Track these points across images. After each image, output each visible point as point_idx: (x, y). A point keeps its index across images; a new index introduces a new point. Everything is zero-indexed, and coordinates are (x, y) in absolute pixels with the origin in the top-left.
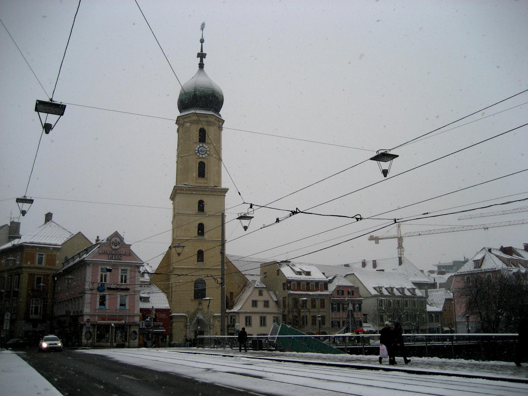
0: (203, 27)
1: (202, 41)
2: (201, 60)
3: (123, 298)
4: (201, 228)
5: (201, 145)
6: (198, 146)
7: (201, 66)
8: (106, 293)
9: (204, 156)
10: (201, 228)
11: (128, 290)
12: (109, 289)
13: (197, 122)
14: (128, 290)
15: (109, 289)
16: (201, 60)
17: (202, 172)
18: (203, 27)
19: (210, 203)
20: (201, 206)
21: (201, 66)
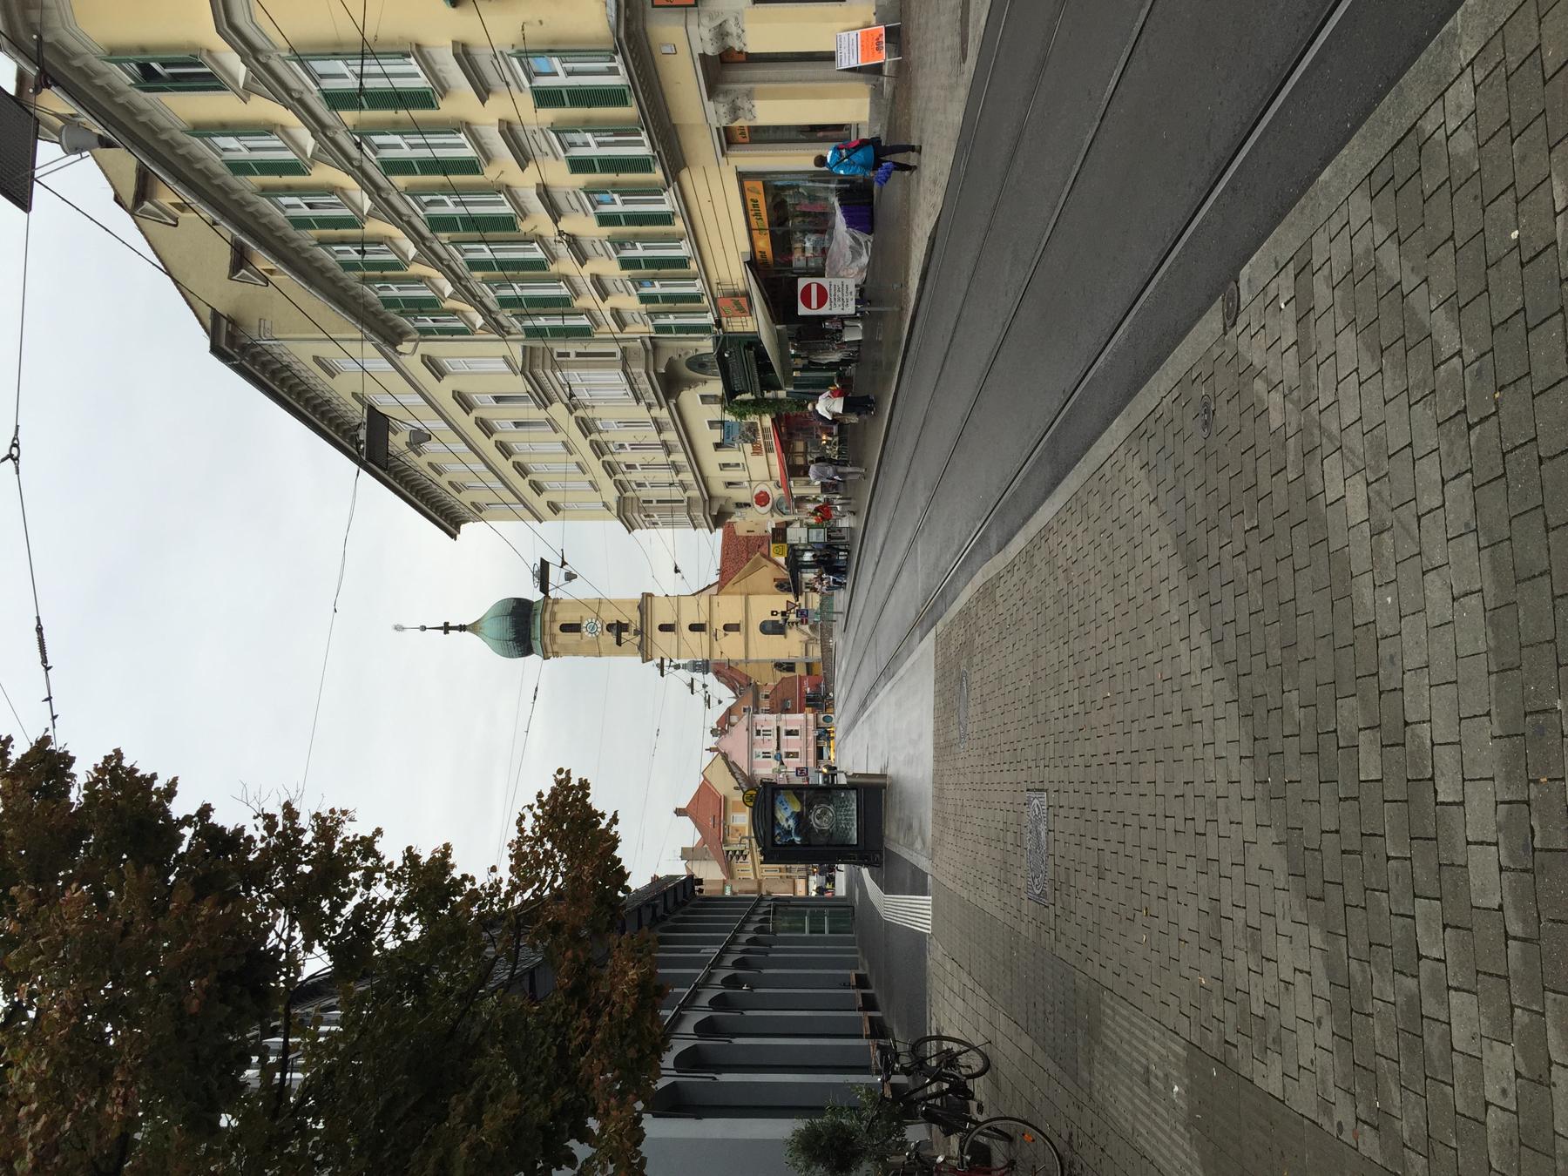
0: (399, 628)
1: (424, 628)
2: (454, 628)
3: (789, 733)
4: (694, 628)
5: (584, 630)
6: (586, 633)
7: (462, 628)
8: (783, 750)
9: (599, 626)
10: (694, 628)
11: (778, 728)
12: (778, 748)
13: (553, 637)
14: (778, 728)
15: (778, 748)
16: (454, 628)
17: (618, 628)
18: (399, 628)
19: (662, 615)
20: (665, 628)
21: (462, 628)
